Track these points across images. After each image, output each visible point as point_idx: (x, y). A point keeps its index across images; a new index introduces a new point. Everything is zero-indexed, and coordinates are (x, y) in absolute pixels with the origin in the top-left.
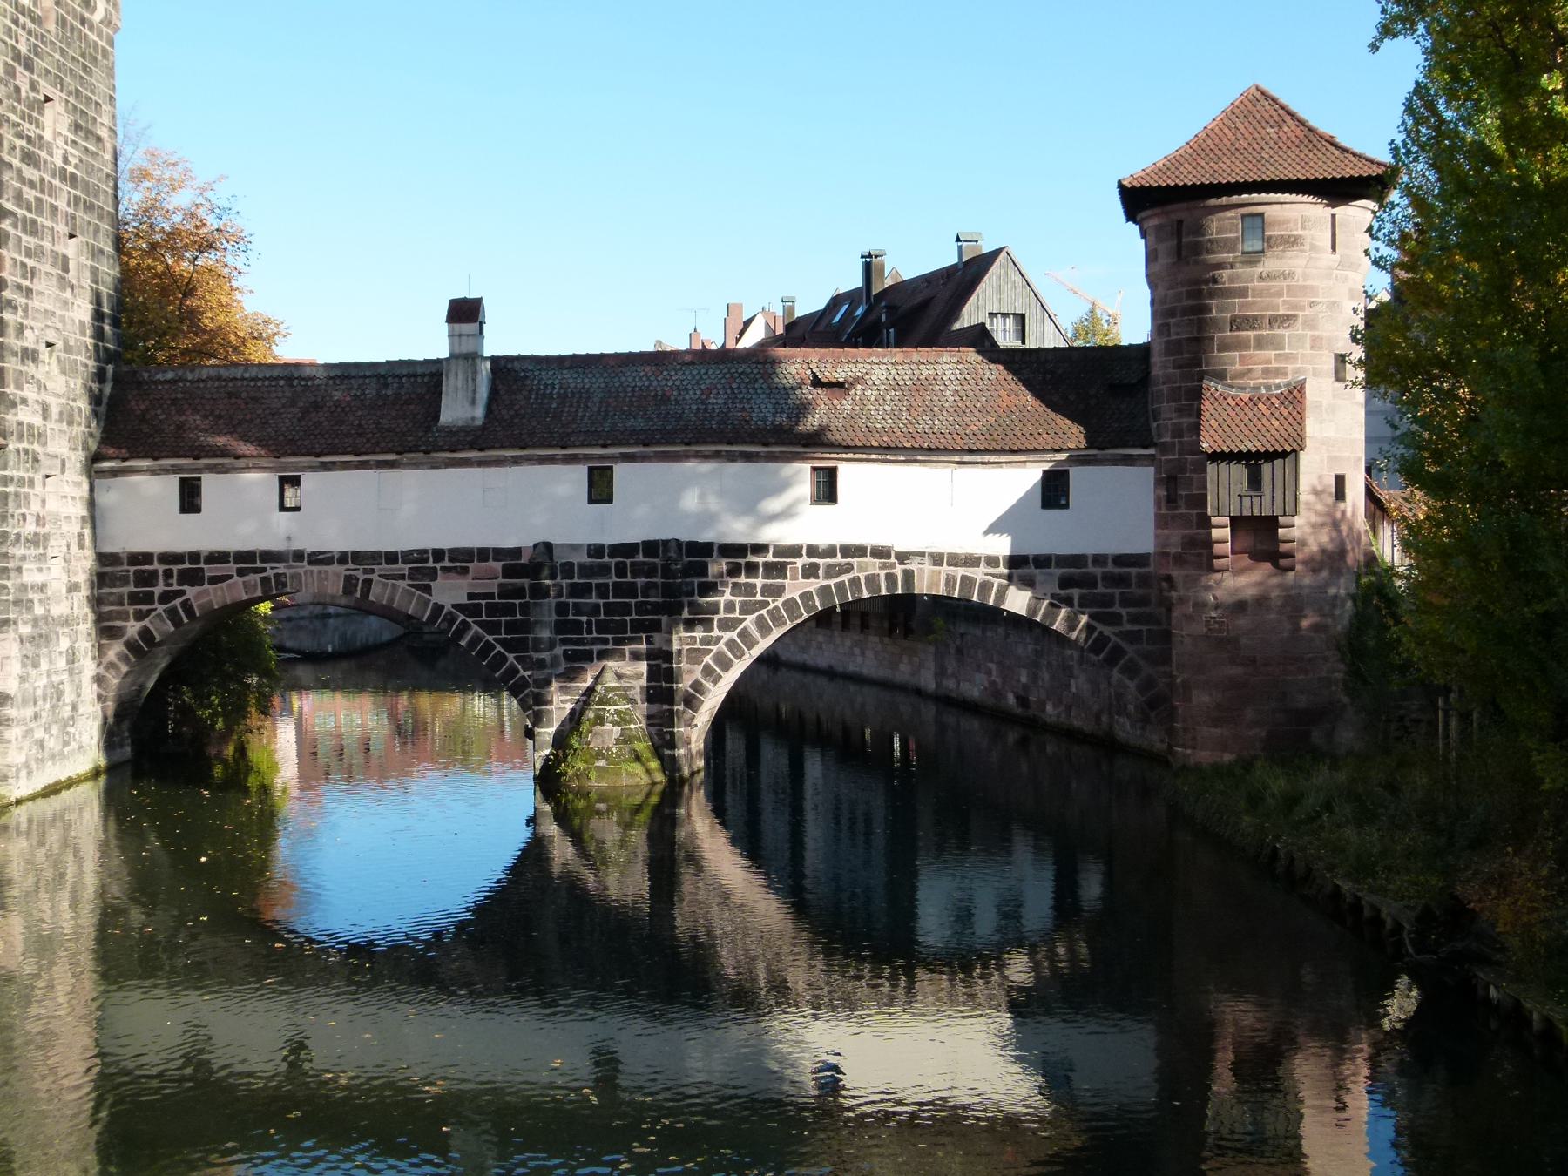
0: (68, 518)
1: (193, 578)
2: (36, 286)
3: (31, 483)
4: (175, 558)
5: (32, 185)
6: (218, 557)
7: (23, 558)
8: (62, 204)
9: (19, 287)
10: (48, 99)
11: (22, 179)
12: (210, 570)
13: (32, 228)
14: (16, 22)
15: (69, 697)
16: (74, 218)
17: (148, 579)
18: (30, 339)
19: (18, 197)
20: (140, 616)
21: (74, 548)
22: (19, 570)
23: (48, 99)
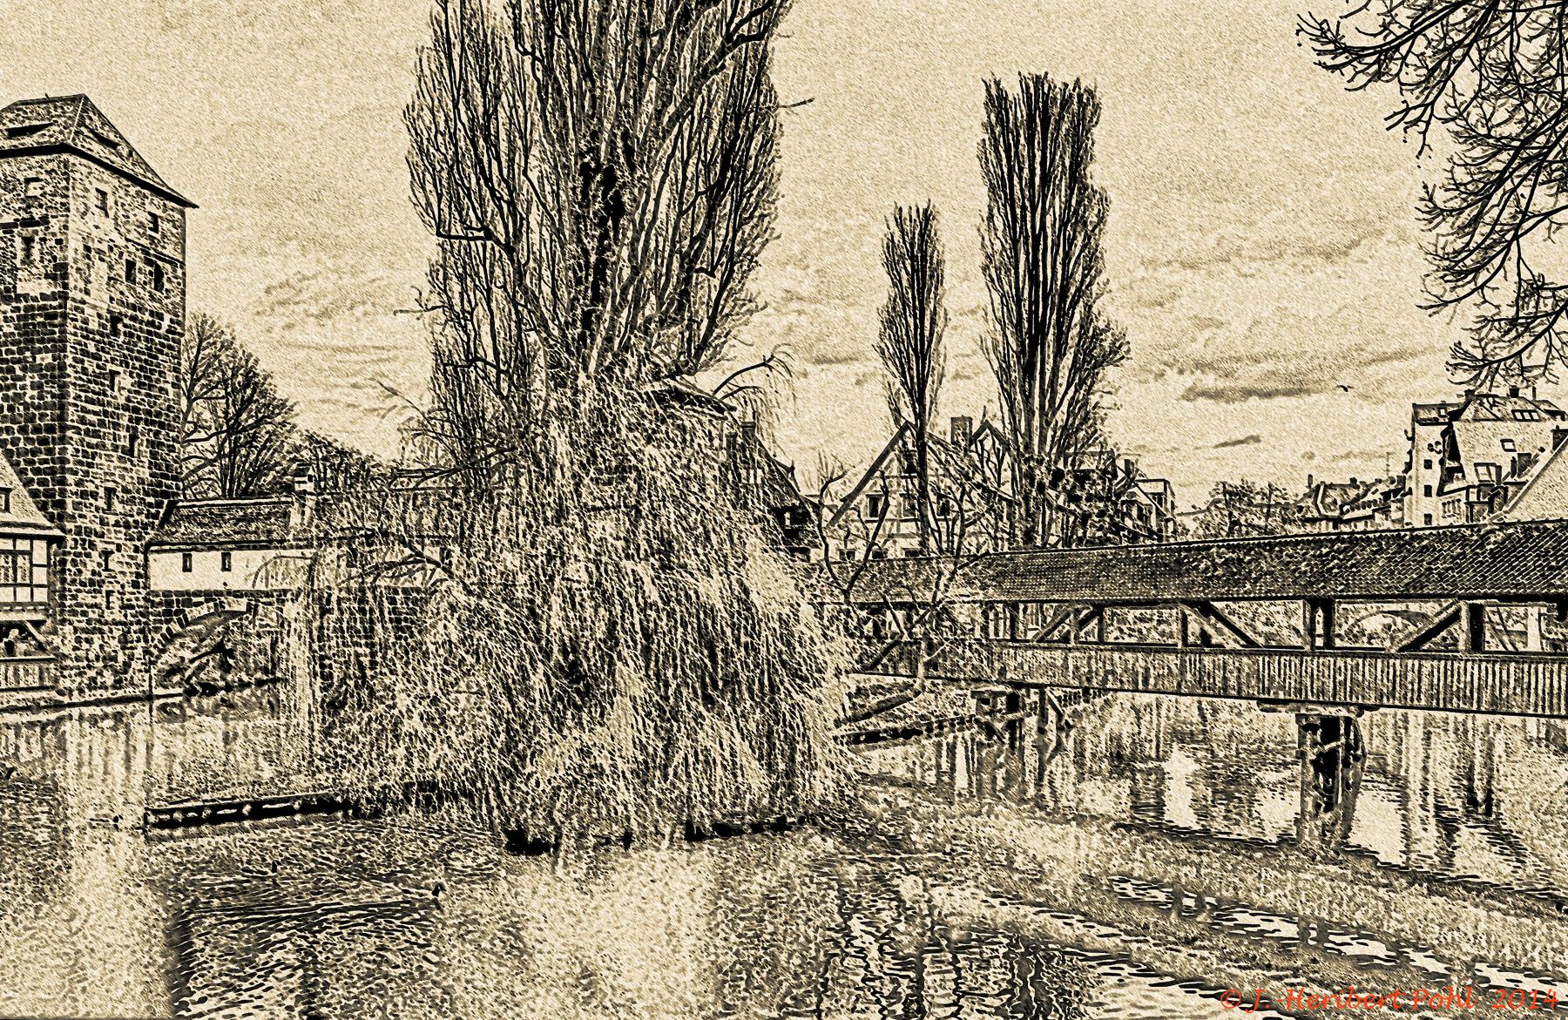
0: (123, 573)
1: (189, 604)
2: (97, 460)
3: (88, 555)
4: (178, 593)
5: (95, 413)
6: (197, 594)
7: (79, 591)
8: (124, 421)
9: (81, 463)
10: (114, 374)
11: (84, 410)
12: (195, 600)
13: (96, 434)
14: (87, 338)
15: (121, 658)
16: (135, 429)
17: (169, 604)
18: (90, 487)
19: (82, 420)
20: (167, 622)
21: (128, 589)
22: (74, 597)
23: (114, 374)
